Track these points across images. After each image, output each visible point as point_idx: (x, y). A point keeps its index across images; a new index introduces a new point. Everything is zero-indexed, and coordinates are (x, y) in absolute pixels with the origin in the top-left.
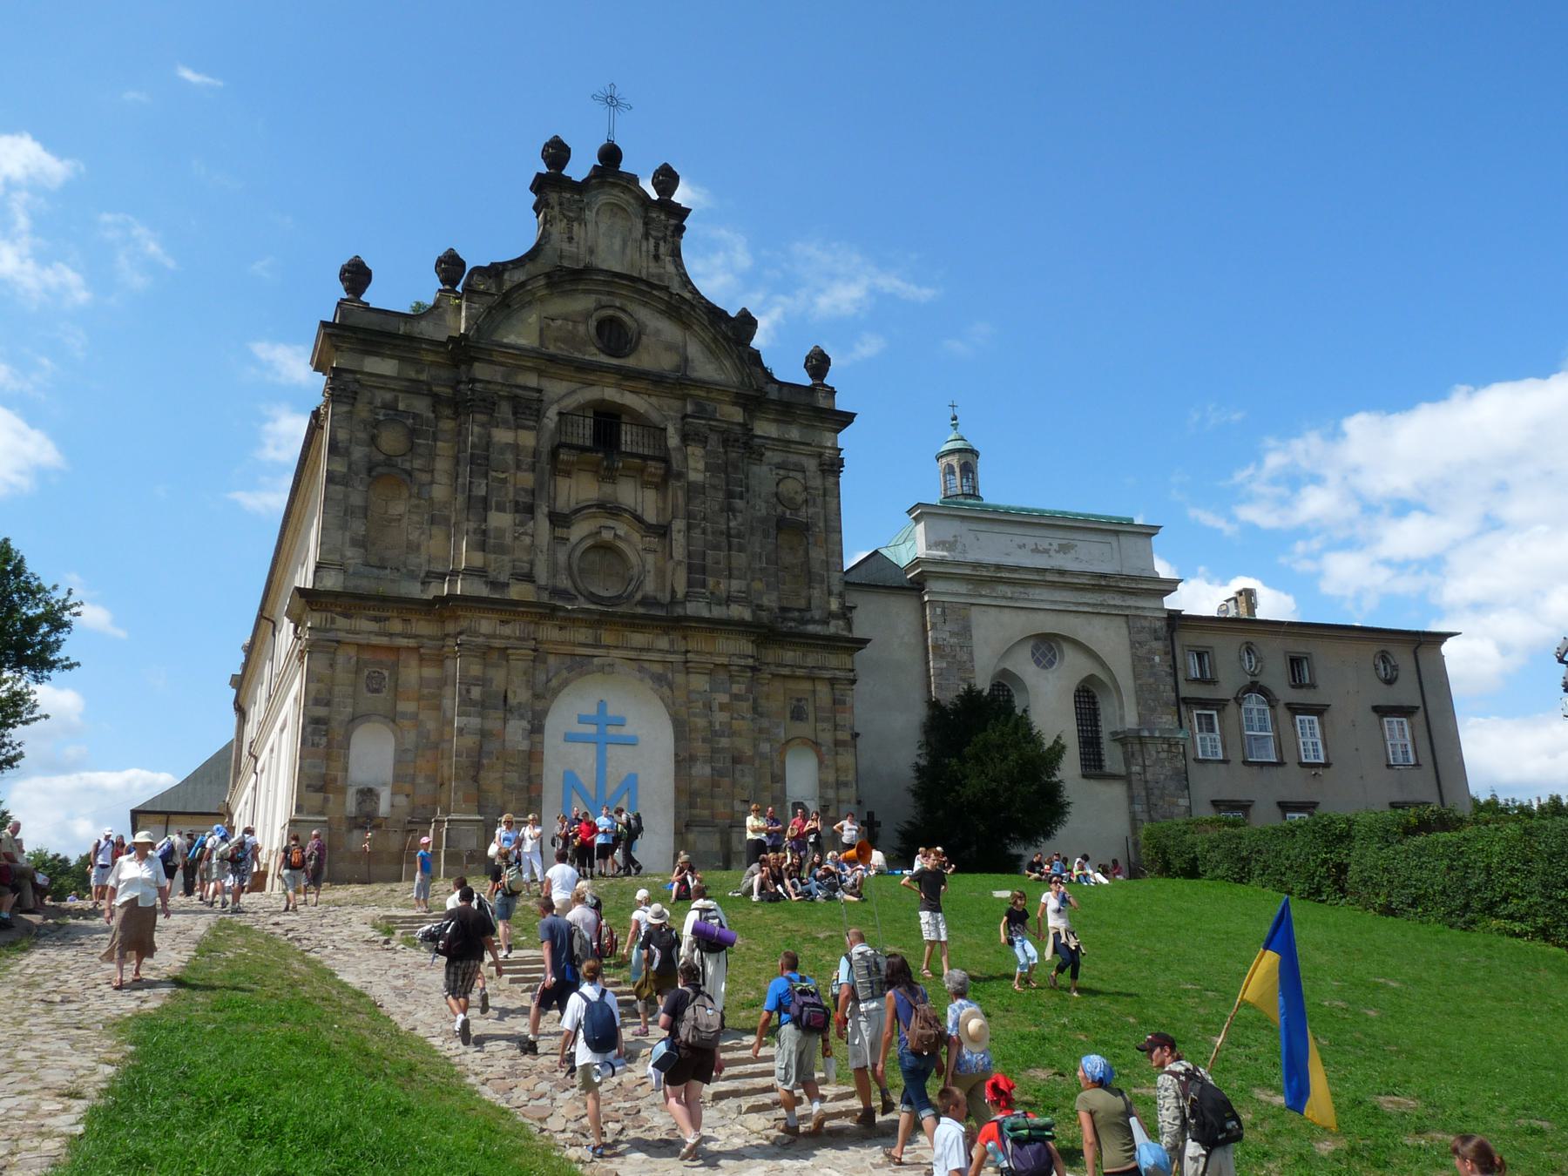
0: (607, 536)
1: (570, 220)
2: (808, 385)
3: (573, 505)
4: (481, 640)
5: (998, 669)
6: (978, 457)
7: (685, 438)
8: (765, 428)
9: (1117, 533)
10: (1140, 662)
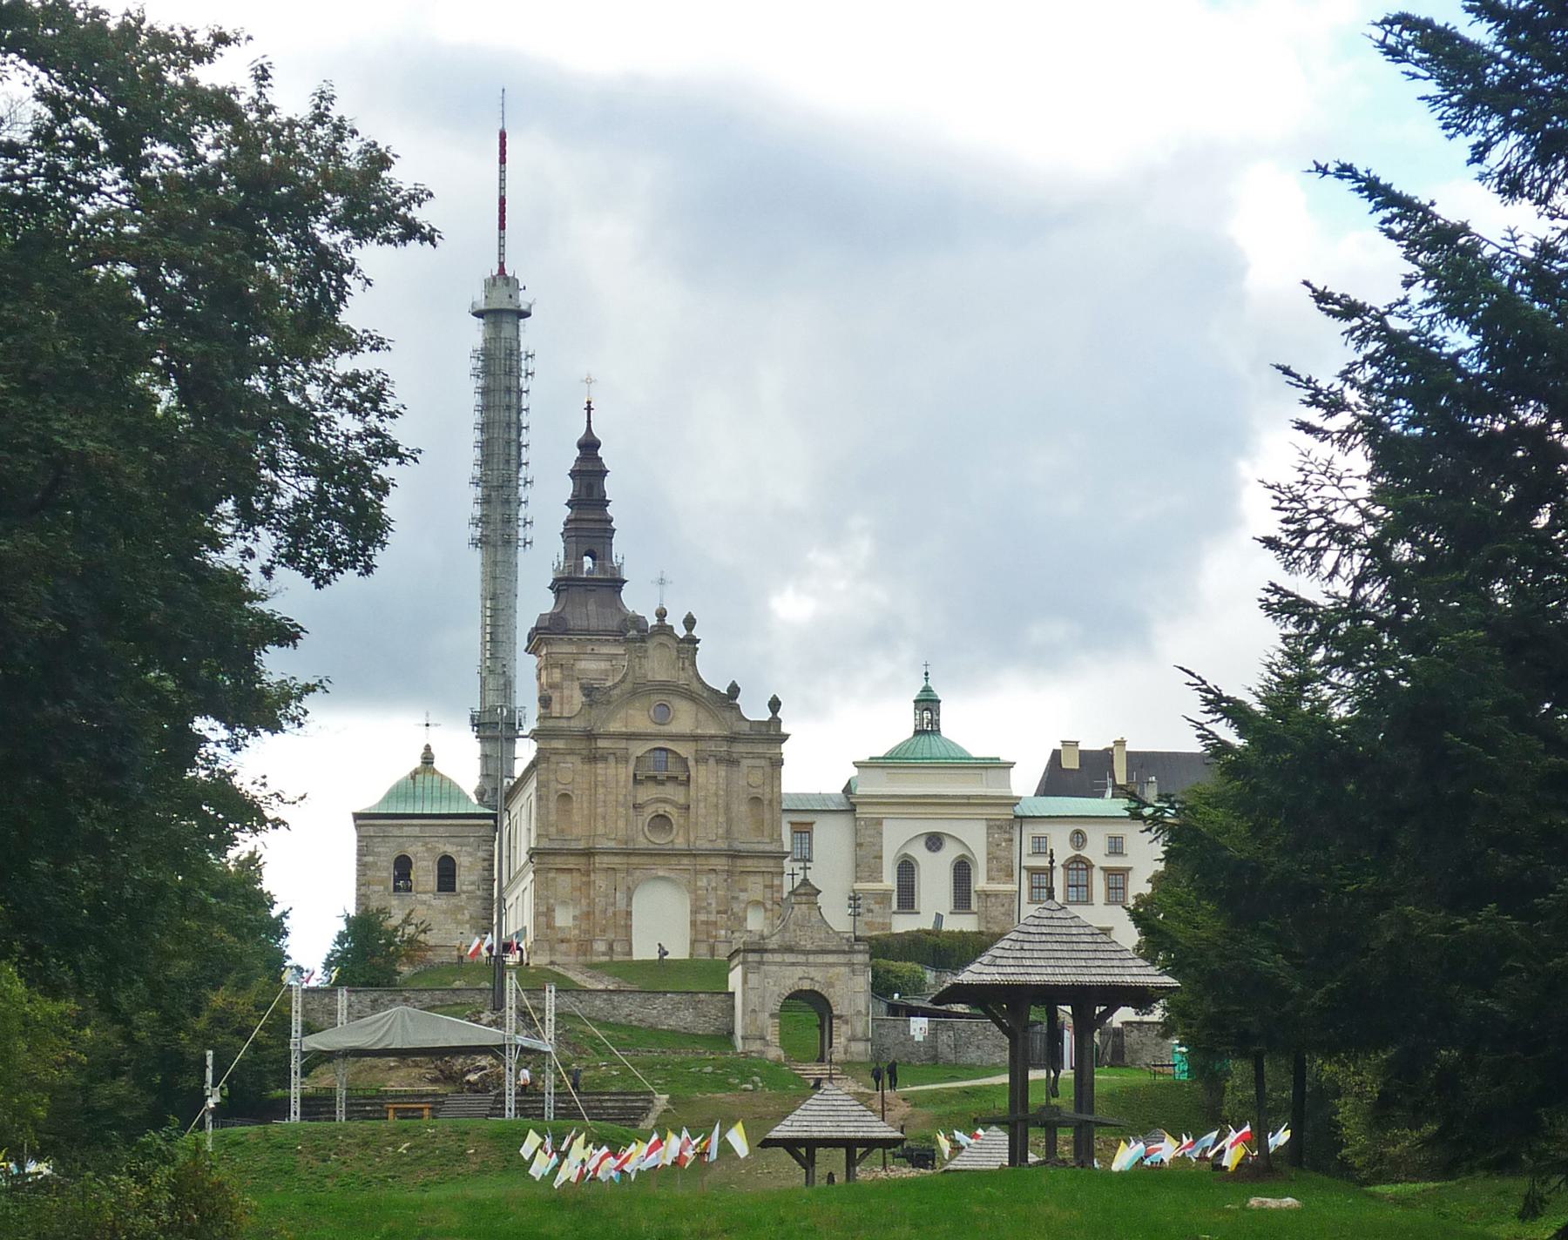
0: (661, 812)
1: (640, 657)
2: (767, 719)
4: (605, 866)
5: (902, 853)
7: (697, 761)
8: (739, 748)
9: (986, 768)
10: (992, 846)
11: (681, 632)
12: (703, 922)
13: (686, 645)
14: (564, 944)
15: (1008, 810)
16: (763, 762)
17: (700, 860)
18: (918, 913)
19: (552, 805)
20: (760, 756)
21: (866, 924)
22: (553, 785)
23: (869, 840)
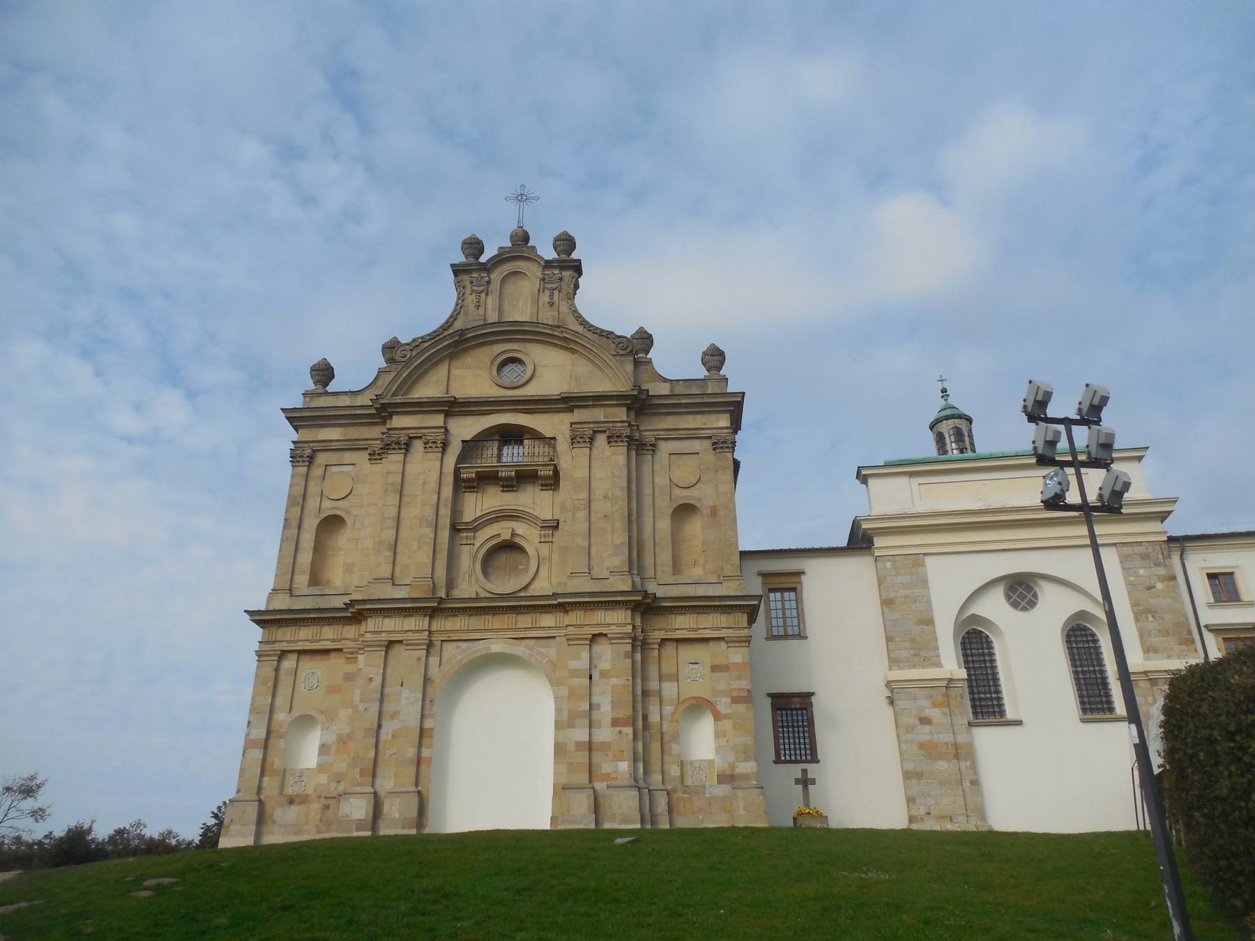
0: (506, 536)
3: (479, 514)
4: (384, 637)
6: (971, 424)
11: (549, 254)
12: (579, 745)
13: (556, 272)
14: (295, 809)
15: (1154, 526)
16: (696, 445)
17: (573, 617)
18: (1018, 723)
19: (308, 538)
20: (692, 435)
21: (922, 746)
22: (312, 503)
23: (905, 592)
